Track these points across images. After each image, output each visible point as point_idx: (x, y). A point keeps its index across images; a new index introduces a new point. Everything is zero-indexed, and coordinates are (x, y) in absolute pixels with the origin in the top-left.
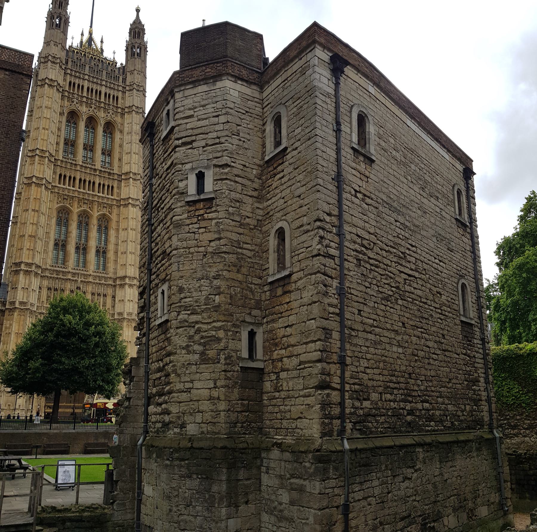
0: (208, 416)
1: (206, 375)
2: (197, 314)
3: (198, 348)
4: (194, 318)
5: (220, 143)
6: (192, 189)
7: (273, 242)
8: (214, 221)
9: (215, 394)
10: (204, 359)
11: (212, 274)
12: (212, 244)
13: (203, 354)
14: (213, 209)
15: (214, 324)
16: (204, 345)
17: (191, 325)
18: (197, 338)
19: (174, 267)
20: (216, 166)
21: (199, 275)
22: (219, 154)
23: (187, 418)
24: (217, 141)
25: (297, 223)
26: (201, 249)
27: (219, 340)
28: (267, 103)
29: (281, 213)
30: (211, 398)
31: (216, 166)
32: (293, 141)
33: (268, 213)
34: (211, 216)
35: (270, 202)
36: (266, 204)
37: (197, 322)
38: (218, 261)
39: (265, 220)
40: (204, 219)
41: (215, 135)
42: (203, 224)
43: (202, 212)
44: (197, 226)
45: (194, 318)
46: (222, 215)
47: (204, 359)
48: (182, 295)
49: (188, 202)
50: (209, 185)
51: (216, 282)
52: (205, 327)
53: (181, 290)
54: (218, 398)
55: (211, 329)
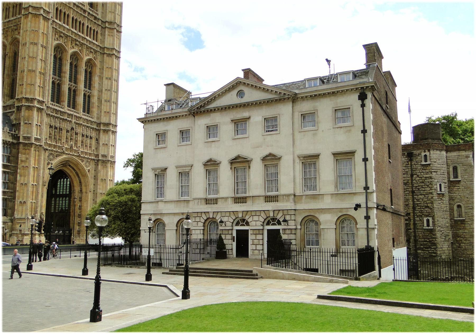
0: (447, 254)
1: (446, 244)
2: (443, 228)
3: (444, 237)
4: (442, 229)
5: (444, 175)
6: (439, 190)
7: (455, 208)
8: (445, 201)
9: (449, 249)
10: (445, 240)
11: (446, 217)
12: (445, 208)
13: (445, 239)
14: (444, 197)
15: (447, 231)
16: (445, 237)
17: (441, 231)
18: (443, 235)
19: (435, 214)
20: (444, 183)
21: (442, 217)
22: (444, 179)
23: (442, 255)
24: (443, 174)
25: (467, 205)
26: (442, 209)
27: (448, 235)
28: (449, 159)
29: (459, 200)
30: (448, 250)
31: (444, 183)
32: (463, 179)
33: (452, 198)
34: (444, 199)
35: (452, 194)
36: (450, 194)
37: (442, 231)
38: (447, 213)
39: (450, 199)
40: (442, 200)
41: (442, 171)
42: (442, 201)
43: (441, 197)
44: (440, 202)
45: (442, 229)
46: (446, 199)
47: (445, 240)
48: (438, 223)
49: (438, 194)
50: (443, 189)
51: (447, 220)
52: (445, 232)
53: (438, 221)
54: (450, 250)
55: (446, 233)
